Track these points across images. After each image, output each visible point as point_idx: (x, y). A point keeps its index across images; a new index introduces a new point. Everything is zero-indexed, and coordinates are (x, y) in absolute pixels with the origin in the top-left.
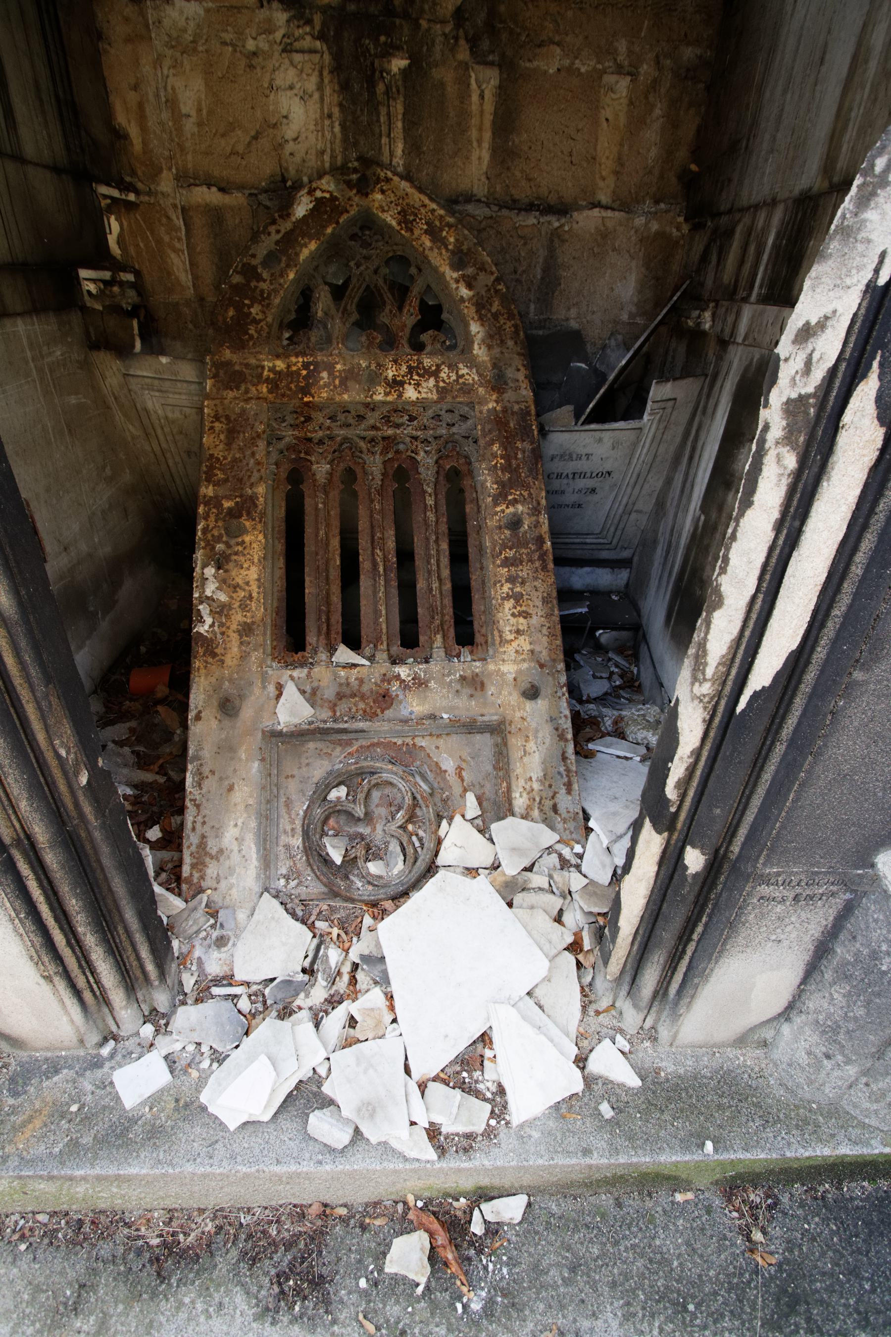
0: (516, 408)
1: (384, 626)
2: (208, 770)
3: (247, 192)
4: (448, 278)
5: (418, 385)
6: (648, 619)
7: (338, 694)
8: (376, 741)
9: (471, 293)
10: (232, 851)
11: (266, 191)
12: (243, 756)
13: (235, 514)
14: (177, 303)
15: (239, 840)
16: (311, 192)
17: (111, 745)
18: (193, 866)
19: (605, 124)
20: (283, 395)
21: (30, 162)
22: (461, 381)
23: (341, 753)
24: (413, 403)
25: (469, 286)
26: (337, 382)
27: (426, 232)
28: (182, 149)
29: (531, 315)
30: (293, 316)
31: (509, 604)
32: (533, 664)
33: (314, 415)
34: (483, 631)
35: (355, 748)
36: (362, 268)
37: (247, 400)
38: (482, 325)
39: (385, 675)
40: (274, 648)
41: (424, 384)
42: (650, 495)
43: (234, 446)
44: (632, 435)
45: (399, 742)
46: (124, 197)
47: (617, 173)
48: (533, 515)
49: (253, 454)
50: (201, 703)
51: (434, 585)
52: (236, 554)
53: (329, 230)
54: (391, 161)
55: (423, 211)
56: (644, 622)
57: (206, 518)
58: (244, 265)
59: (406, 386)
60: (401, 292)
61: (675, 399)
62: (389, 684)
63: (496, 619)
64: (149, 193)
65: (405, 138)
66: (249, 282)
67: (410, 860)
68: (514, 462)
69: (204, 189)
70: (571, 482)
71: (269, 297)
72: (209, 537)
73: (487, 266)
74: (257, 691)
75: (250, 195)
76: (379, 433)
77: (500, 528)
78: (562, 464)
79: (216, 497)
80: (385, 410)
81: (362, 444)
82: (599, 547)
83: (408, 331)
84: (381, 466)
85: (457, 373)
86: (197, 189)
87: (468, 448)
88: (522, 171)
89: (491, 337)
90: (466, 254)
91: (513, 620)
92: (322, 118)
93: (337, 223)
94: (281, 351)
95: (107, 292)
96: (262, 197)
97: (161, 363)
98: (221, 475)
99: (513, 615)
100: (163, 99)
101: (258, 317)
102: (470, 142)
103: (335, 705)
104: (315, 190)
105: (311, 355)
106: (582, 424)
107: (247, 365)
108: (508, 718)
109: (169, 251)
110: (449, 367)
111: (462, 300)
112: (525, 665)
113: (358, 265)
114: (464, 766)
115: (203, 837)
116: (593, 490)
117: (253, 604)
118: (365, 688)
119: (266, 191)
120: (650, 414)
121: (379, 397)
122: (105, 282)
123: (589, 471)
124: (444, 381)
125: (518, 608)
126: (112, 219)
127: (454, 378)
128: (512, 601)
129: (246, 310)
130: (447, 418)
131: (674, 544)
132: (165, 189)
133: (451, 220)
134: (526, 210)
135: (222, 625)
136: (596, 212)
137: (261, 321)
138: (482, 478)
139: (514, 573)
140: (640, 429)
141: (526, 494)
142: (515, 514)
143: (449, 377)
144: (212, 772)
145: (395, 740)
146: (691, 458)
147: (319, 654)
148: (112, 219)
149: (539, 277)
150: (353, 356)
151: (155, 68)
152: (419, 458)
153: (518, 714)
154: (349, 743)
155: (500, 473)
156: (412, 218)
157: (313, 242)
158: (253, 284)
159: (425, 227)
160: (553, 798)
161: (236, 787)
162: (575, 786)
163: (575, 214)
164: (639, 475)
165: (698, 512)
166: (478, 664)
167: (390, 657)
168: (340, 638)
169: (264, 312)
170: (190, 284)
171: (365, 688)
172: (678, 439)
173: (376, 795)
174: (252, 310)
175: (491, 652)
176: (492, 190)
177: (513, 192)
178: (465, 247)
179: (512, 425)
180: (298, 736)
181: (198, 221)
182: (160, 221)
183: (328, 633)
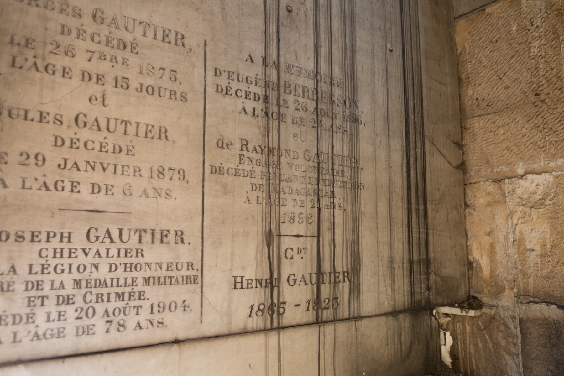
28: (525, 275)
46: (464, 313)
64: (491, 307)
69: (544, 305)
86: (535, 305)
100: (512, 240)
109: (504, 353)
126: (448, 334)
132: (506, 304)
148: (448, 334)
151: (507, 220)
181: (535, 331)
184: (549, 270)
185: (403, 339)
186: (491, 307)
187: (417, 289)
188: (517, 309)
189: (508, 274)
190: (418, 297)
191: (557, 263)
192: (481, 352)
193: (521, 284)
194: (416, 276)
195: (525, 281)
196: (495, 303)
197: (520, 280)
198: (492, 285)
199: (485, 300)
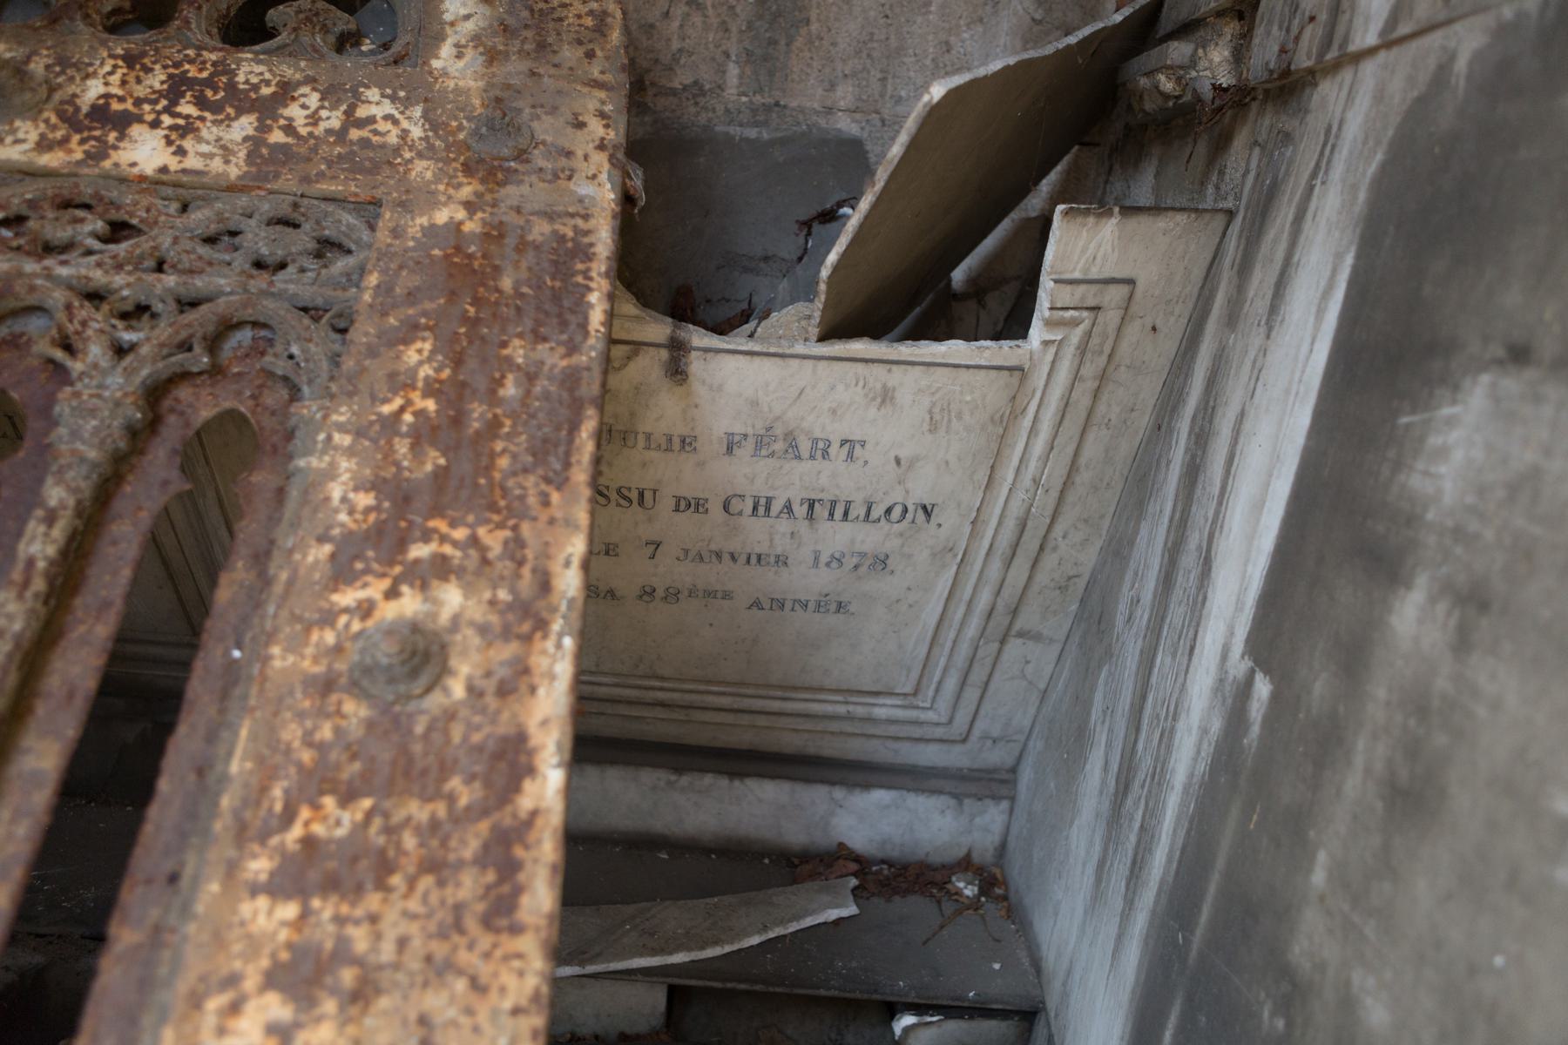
0: (540, 230)
5: (188, 129)
6: (1065, 995)
22: (355, 134)
29: (731, 91)
41: (209, 131)
42: (1062, 589)
44: (992, 390)
48: (507, 634)
56: (1051, 1004)
59: (136, 130)
61: (1131, 282)
68: (477, 413)
70: (803, 526)
77: (326, 686)
78: (764, 466)
82: (917, 732)
85: (349, 113)
87: (306, 346)
106: (823, 338)
120: (1049, 324)
123: (858, 498)
124: (289, 129)
131: (1146, 764)
139: (324, 932)
143: (314, 119)
146: (1193, 472)
152: (77, 366)
155: (402, 447)
164: (1022, 526)
165: (1239, 665)
172: (1144, 420)
179: (507, 283)
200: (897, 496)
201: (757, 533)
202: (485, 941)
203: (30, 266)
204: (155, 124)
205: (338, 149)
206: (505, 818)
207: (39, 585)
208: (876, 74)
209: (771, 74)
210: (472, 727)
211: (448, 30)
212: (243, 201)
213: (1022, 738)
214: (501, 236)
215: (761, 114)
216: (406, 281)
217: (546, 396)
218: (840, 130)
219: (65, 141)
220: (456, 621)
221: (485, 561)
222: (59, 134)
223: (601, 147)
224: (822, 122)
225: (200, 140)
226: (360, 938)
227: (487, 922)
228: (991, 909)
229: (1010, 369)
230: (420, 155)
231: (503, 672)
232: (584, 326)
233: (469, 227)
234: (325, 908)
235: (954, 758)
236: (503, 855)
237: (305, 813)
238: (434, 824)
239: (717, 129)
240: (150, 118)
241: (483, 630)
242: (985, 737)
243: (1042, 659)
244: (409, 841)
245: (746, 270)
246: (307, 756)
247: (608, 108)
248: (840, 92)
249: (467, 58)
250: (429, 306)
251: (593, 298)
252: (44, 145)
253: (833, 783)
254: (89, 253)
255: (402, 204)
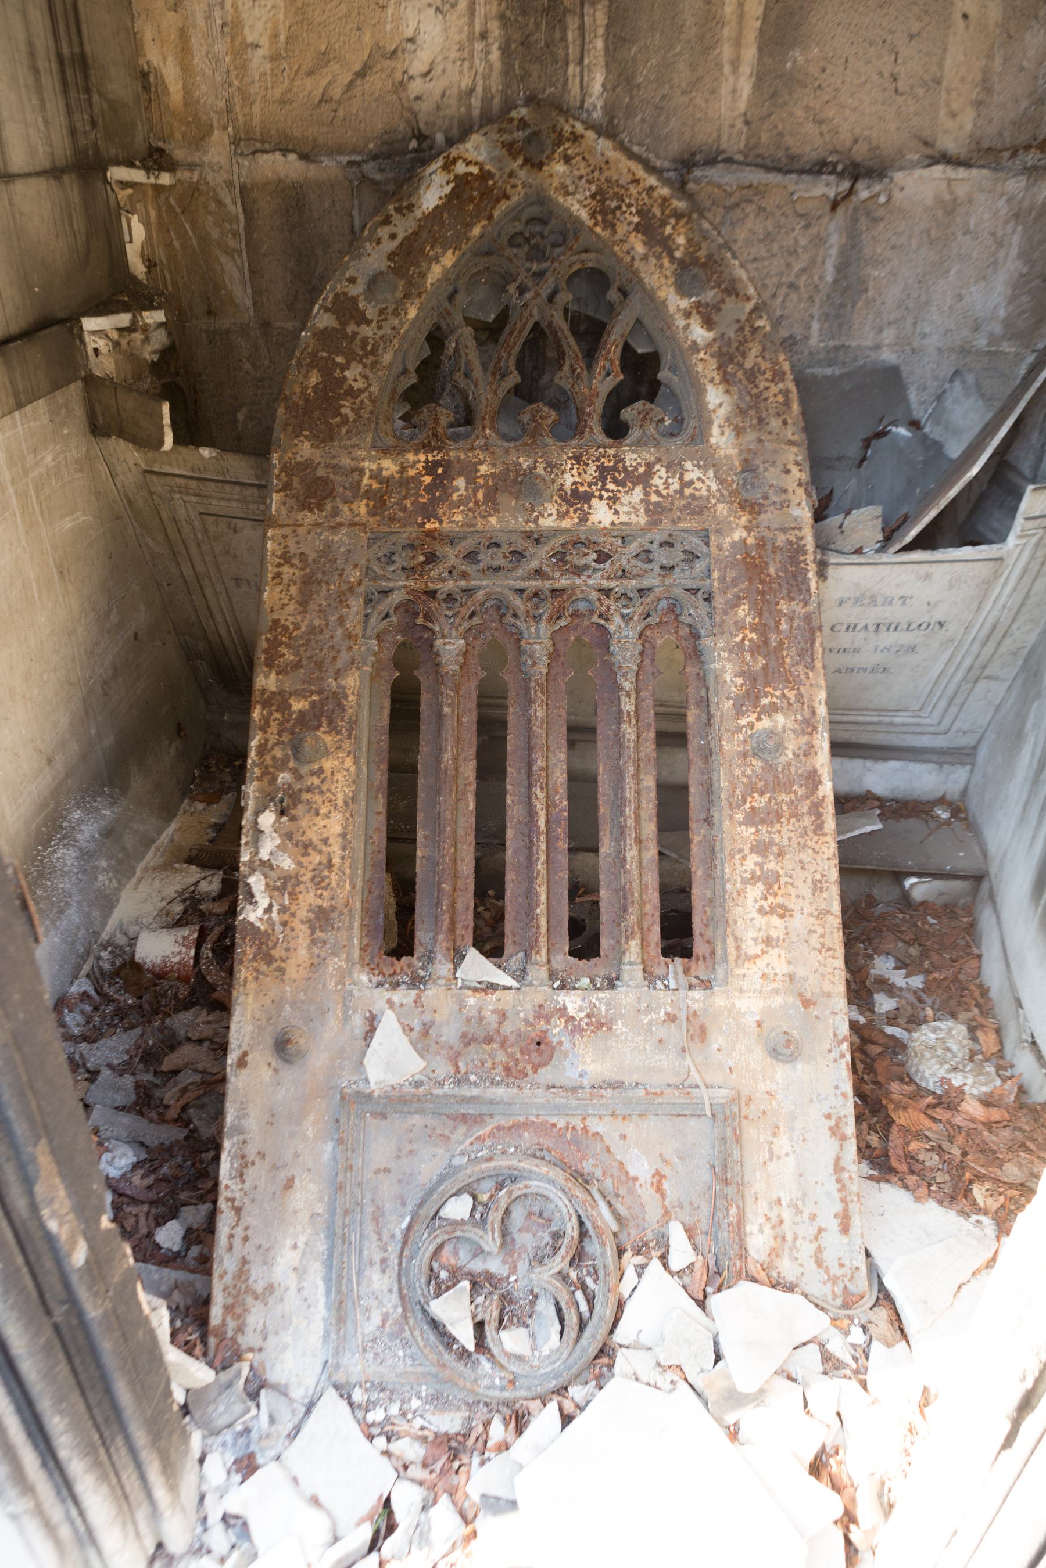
0: (781, 539)
1: (543, 921)
2: (254, 1151)
3: (344, 159)
4: (672, 309)
5: (614, 499)
6: (1001, 867)
7: (464, 1035)
8: (522, 1119)
9: (710, 335)
10: (287, 1289)
11: (374, 158)
12: (310, 1133)
13: (307, 722)
14: (228, 331)
15: (300, 1271)
16: (447, 167)
17: (106, 1074)
18: (228, 1309)
19: (961, 23)
20: (392, 519)
21: (19, 176)
22: (687, 492)
23: (466, 1136)
24: (606, 532)
25: (708, 323)
26: (480, 495)
27: (637, 228)
28: (245, 97)
29: (813, 341)
30: (413, 379)
31: (755, 892)
32: (790, 1000)
33: (441, 550)
34: (709, 933)
35: (488, 1129)
36: (528, 295)
37: (335, 528)
38: (727, 392)
39: (541, 1006)
40: (363, 949)
41: (625, 499)
43: (312, 606)
44: (984, 570)
45: (561, 1124)
46: (152, 180)
47: (979, 104)
48: (803, 732)
49: (341, 620)
50: (247, 1039)
51: (631, 864)
52: (308, 790)
53: (476, 231)
54: (583, 102)
55: (633, 190)
56: (993, 871)
57: (264, 729)
58: (337, 295)
59: (594, 502)
60: (591, 333)
62: (548, 1022)
63: (730, 917)
64: (191, 166)
65: (607, 65)
66: (344, 324)
67: (571, 1332)
68: (773, 638)
69: (278, 155)
70: (871, 635)
71: (373, 352)
72: (268, 760)
73: (739, 287)
74: (333, 1022)
75: (350, 163)
76: (547, 584)
77: (745, 755)
79: (281, 692)
80: (557, 542)
81: (518, 603)
82: (919, 730)
83: (599, 404)
84: (548, 643)
85: (681, 478)
86: (265, 157)
88: (807, 108)
89: (741, 412)
90: (704, 266)
91: (760, 921)
92: (471, 38)
93: (490, 217)
94: (391, 441)
95: (124, 342)
96: (369, 168)
97: (202, 457)
98: (289, 657)
99: (761, 911)
100: (219, 22)
101: (356, 386)
102: (719, 66)
103: (458, 1054)
104: (455, 161)
105: (440, 449)
107: (336, 468)
108: (745, 1092)
110: (669, 467)
111: (695, 347)
112: (778, 1001)
113: (522, 290)
114: (666, 1171)
115: (244, 1261)
116: (912, 649)
117: (333, 876)
118: (507, 1029)
119: (374, 158)
121: (548, 522)
122: (120, 330)
124: (658, 493)
125: (771, 899)
126: (135, 219)
127: (676, 486)
128: (760, 886)
129: (337, 373)
130: (661, 557)
132: (216, 159)
133: (680, 205)
134: (809, 172)
135: (283, 909)
136: (938, 170)
137: (361, 391)
138: (717, 666)
139: (765, 837)
140: (1000, 559)
141: (791, 695)
142: (771, 733)
144: (262, 1155)
145: (553, 1120)
147: (437, 966)
148: (135, 219)
149: (829, 279)
150: (507, 452)
152: (612, 628)
153: (762, 1087)
154: (478, 1120)
155: (748, 656)
156: (614, 204)
157: (450, 252)
158: (351, 328)
159: (636, 219)
160: (816, 1238)
161: (297, 1181)
162: (856, 1222)
163: (898, 176)
164: (994, 627)
166: (697, 994)
167: (552, 975)
168: (469, 939)
169: (366, 377)
170: (249, 302)
171: (507, 1029)
173: (518, 1216)
174: (347, 373)
175: (720, 972)
176: (753, 141)
177: (789, 140)
178: (702, 254)
179: (772, 571)
180: (398, 1102)
182: (205, 207)
183: (452, 929)
184: (285, 86)
185: (76, 227)
186: (191, 166)
187: (79, 125)
188: (235, 168)
189: (217, 97)
190: (82, 141)
191: (297, 72)
192: (180, 257)
193: (240, 117)
194: (73, 94)
195: (246, 110)
196: (196, 158)
197: (238, 108)
198: (188, 123)
199: (179, 154)
200: (926, 619)
201: (845, 639)
202: (816, 838)
203: (578, 582)
204: (601, 498)
205: (682, 502)
206: (815, 798)
207: (634, 721)
208: (910, 320)
209: (840, 326)
210: (797, 768)
211: (714, 416)
212: (649, 536)
213: (982, 731)
214: (764, 545)
215: (831, 357)
216: (731, 574)
217: (799, 627)
218: (883, 361)
219: (568, 512)
220: (784, 727)
221: (790, 704)
222: (564, 508)
223: (800, 485)
224: (873, 355)
225: (622, 504)
226: (776, 838)
227: (815, 832)
228: (957, 825)
229: (996, 559)
230: (718, 501)
231: (804, 747)
232: (808, 590)
233: (750, 541)
234: (764, 829)
235: (940, 742)
236: (816, 810)
237: (749, 799)
238: (792, 802)
239: (808, 371)
240: (597, 494)
241: (794, 731)
242: (959, 731)
243: (998, 690)
244: (785, 808)
245: (828, 468)
246: (745, 780)
247: (800, 458)
248: (885, 333)
249: (726, 434)
250: (742, 586)
251: (810, 575)
252: (561, 516)
253: (866, 758)
254: (595, 570)
255: (718, 531)
